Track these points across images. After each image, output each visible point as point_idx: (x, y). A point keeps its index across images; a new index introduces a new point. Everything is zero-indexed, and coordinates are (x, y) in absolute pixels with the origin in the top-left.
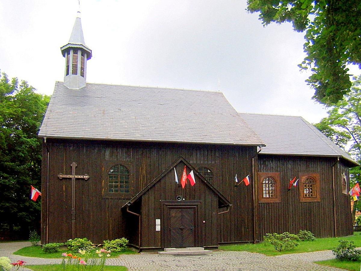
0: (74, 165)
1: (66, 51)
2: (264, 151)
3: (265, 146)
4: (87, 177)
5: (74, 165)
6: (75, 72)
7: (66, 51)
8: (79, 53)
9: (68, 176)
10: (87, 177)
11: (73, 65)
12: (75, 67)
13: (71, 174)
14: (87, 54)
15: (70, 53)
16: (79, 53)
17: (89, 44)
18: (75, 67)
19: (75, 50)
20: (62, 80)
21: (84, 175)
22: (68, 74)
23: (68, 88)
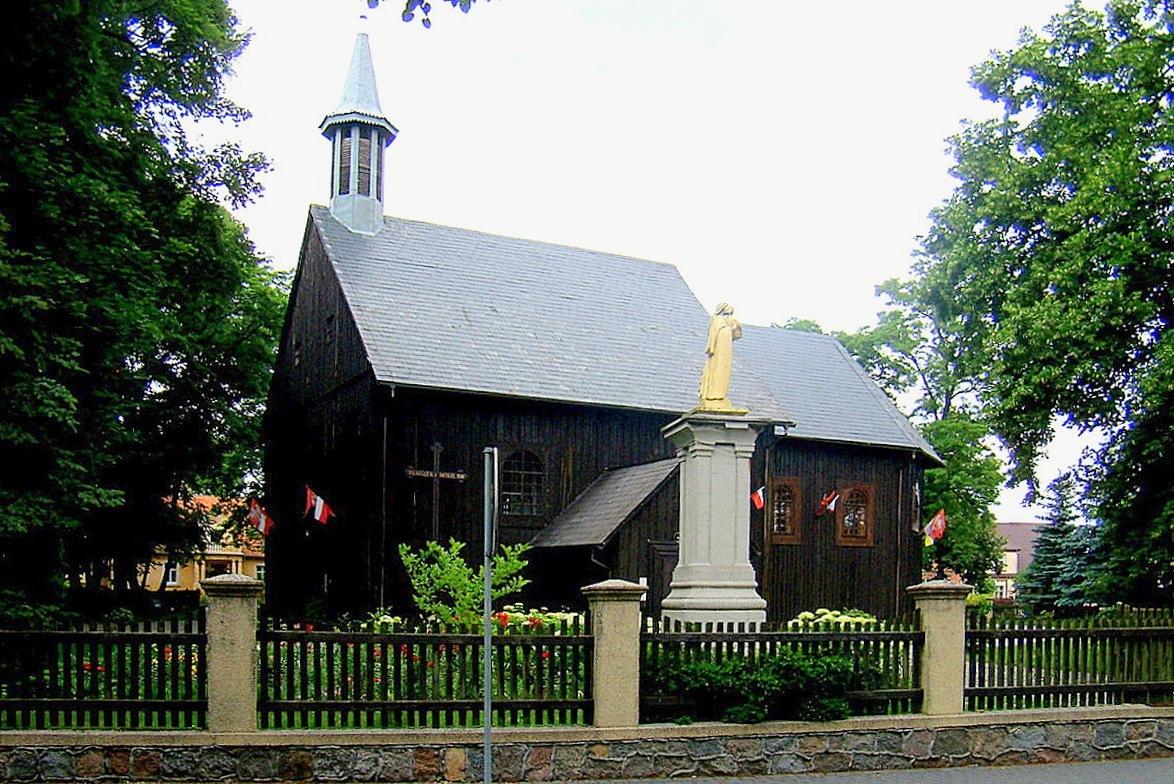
0: (437, 449)
1: (337, 129)
2: (792, 433)
3: (794, 426)
4: (462, 477)
5: (437, 449)
6: (364, 189)
7: (337, 129)
8: (374, 136)
9: (426, 474)
10: (462, 477)
11: (359, 167)
12: (364, 172)
13: (432, 470)
14: (386, 135)
15: (353, 135)
16: (374, 136)
17: (389, 108)
18: (364, 172)
19: (366, 129)
20: (324, 200)
21: (456, 472)
22: (344, 189)
23: (350, 229)
